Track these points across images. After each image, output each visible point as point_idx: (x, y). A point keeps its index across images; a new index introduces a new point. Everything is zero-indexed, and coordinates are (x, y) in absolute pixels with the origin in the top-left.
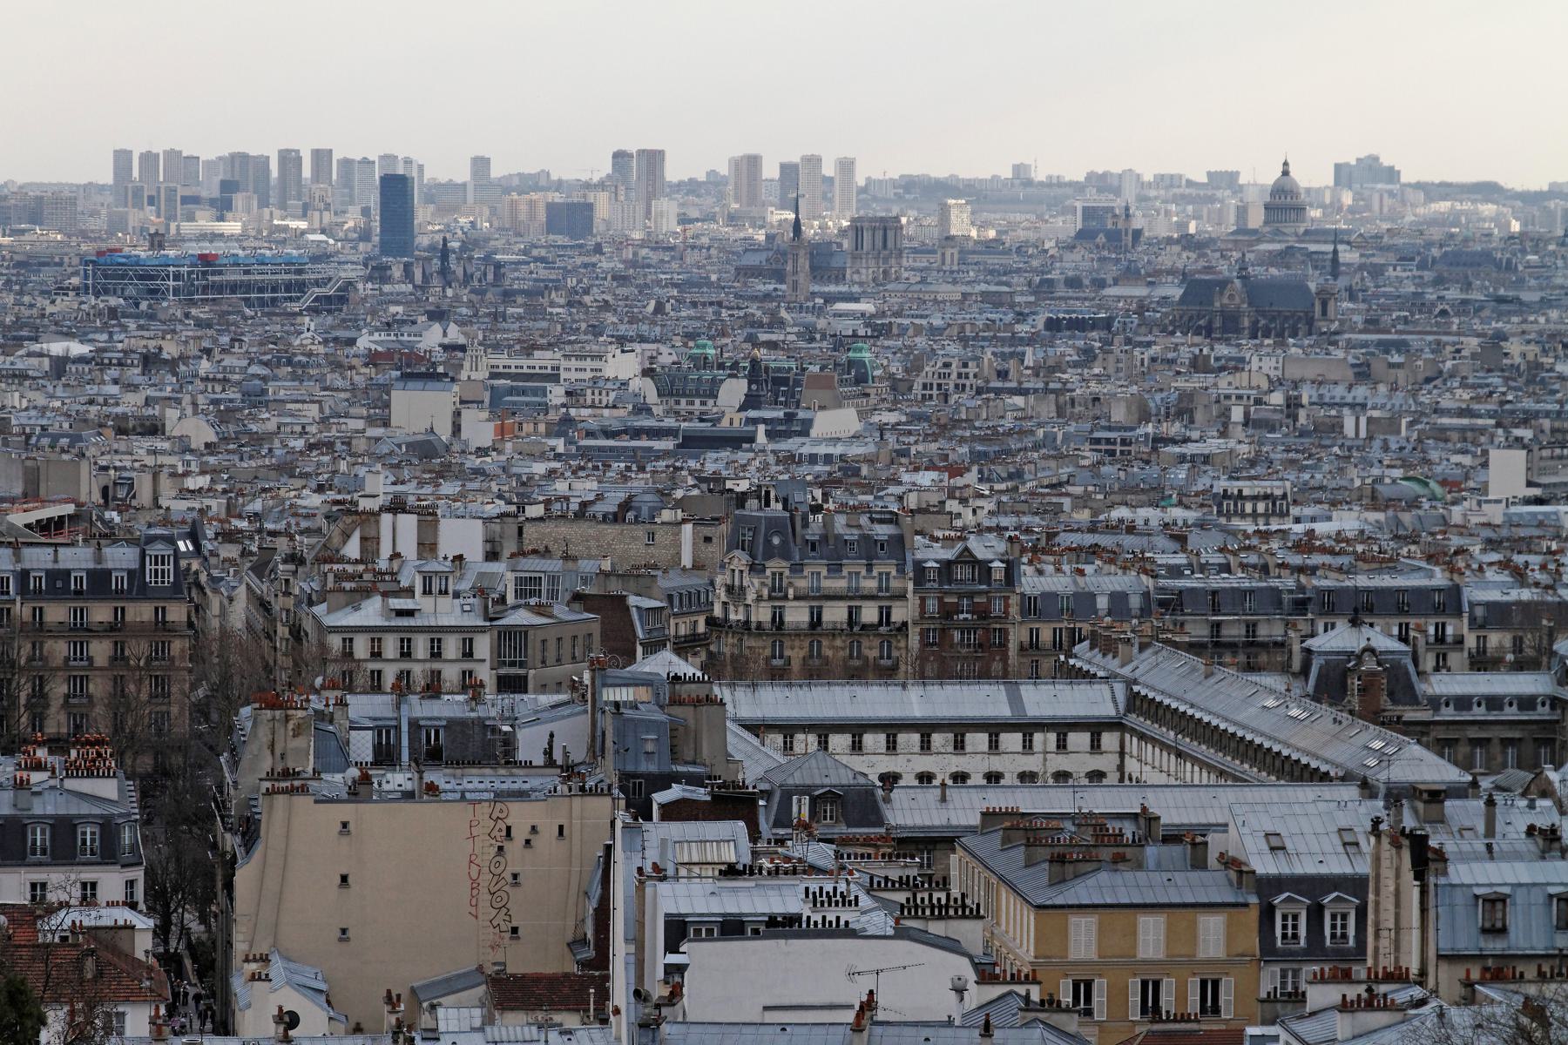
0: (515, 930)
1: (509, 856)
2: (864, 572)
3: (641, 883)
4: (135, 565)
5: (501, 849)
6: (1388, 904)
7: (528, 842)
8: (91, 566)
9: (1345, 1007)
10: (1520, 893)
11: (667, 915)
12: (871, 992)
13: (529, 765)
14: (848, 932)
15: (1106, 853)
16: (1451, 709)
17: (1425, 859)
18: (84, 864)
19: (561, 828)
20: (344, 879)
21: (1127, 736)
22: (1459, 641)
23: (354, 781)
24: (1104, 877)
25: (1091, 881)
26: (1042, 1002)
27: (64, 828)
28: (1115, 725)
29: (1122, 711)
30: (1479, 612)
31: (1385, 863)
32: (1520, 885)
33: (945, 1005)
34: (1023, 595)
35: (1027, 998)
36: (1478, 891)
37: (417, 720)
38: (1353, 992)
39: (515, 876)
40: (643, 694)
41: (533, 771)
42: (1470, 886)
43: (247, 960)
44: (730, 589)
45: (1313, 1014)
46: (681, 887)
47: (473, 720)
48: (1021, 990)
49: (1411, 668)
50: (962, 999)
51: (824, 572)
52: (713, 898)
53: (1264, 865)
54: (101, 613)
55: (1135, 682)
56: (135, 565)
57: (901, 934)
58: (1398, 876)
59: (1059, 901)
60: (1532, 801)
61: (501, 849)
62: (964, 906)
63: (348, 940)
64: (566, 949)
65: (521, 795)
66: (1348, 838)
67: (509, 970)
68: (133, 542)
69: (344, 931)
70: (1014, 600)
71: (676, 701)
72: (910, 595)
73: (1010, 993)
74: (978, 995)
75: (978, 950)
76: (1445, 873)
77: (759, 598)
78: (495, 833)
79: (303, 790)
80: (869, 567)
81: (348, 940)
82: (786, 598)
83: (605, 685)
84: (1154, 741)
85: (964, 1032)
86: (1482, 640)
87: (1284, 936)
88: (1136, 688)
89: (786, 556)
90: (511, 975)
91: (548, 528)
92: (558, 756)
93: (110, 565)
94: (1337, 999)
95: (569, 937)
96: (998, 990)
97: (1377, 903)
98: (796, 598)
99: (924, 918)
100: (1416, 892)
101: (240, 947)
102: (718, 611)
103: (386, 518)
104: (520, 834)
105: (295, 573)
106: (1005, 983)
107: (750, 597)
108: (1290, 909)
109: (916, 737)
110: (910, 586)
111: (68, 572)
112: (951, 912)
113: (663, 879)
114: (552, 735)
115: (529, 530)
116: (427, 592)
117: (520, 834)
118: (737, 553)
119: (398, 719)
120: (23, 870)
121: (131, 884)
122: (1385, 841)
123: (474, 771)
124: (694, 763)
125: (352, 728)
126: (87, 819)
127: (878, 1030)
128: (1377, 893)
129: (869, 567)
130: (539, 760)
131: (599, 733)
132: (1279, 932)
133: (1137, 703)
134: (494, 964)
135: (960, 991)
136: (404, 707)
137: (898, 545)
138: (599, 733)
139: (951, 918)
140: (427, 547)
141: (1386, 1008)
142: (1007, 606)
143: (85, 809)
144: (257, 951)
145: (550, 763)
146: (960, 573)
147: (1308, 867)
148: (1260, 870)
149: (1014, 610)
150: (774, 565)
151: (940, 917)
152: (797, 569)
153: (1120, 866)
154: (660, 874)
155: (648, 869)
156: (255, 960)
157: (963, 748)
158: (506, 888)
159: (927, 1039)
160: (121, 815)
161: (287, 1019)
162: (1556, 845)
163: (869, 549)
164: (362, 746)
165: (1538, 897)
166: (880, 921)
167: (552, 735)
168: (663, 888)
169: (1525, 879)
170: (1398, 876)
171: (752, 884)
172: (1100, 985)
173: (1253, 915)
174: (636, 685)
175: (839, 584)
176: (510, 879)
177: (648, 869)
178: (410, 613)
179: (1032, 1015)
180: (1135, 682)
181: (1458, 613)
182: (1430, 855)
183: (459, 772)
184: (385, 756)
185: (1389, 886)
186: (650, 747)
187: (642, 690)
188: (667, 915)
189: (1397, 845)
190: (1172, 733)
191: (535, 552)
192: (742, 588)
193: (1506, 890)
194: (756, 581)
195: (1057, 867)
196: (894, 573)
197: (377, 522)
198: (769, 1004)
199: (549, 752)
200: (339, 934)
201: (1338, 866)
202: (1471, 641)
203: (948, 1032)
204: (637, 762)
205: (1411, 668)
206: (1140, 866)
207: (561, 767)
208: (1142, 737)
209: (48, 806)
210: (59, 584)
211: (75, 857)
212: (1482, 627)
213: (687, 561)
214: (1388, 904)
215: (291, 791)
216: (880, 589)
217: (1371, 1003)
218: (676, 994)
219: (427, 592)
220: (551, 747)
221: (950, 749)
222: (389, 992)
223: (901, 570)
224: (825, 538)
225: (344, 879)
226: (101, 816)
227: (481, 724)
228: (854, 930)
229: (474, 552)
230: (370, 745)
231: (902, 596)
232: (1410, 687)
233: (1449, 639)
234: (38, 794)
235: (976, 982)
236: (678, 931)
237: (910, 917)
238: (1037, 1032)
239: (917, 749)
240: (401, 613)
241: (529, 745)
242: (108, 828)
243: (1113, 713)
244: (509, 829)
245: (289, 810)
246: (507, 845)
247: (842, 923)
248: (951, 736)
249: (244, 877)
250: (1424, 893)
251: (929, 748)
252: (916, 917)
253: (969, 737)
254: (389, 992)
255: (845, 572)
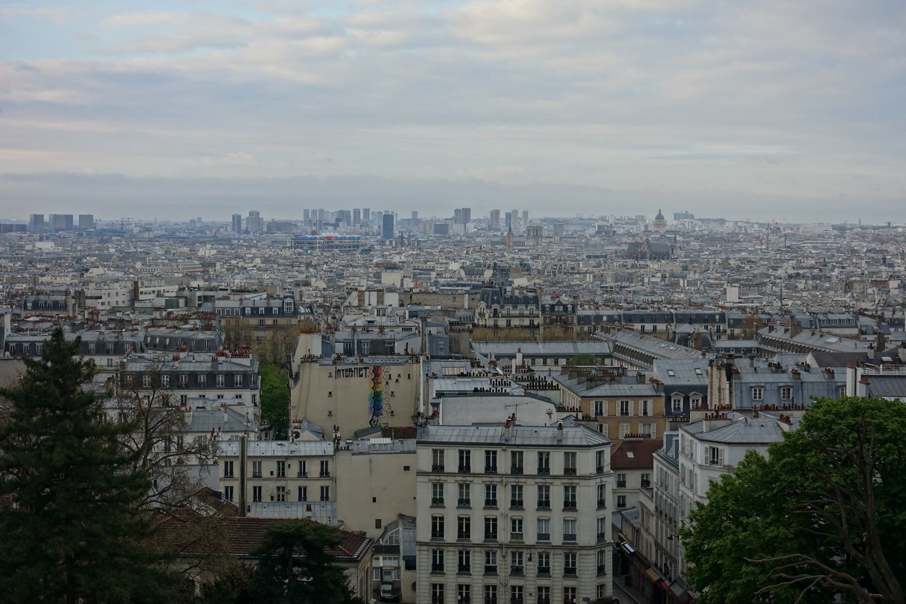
0: (392, 412)
1: (390, 385)
2: (525, 308)
3: (427, 380)
4: (281, 306)
5: (387, 383)
6: (716, 392)
7: (397, 380)
8: (266, 306)
9: (707, 418)
10: (768, 385)
11: (436, 391)
12: (514, 414)
13: (399, 354)
14: (506, 394)
15: (607, 379)
16: (723, 352)
17: (731, 373)
18: (237, 389)
19: (409, 375)
20: (330, 393)
21: (614, 360)
22: (725, 331)
23: (335, 359)
24: (607, 386)
25: (602, 388)
26: (583, 417)
27: (229, 375)
28: (609, 356)
29: (612, 350)
30: (731, 322)
31: (715, 376)
32: (768, 383)
33: (543, 419)
34: (578, 316)
35: (577, 417)
36: (751, 385)
37: (361, 340)
38: (709, 413)
39: (392, 393)
40: (441, 329)
41: (400, 357)
42: (749, 383)
43: (294, 422)
44: (480, 314)
45: (692, 423)
46: (442, 381)
47: (380, 340)
48: (574, 414)
49: (710, 339)
50: (551, 417)
51: (511, 308)
52: (455, 385)
53: (668, 382)
54: (269, 321)
55: (616, 341)
56: (281, 306)
57: (527, 395)
58: (720, 381)
59: (590, 394)
60: (767, 359)
61: (387, 383)
62: (552, 386)
63: (331, 416)
64: (411, 419)
65: (396, 364)
66: (698, 371)
67: (389, 426)
68: (280, 299)
69: (330, 412)
70: (575, 318)
71: (452, 330)
72: (540, 316)
73: (570, 416)
74: (557, 417)
75: (557, 402)
76: (739, 378)
77: (490, 317)
78: (385, 377)
79: (316, 361)
80: (527, 307)
81: (331, 416)
82: (498, 317)
83: (426, 326)
84: (623, 360)
85: (551, 429)
86: (732, 331)
87: (675, 408)
88: (616, 343)
89: (498, 303)
90: (389, 428)
91: (421, 296)
92: (409, 351)
93: (272, 306)
94: (704, 416)
95: (412, 414)
96: (565, 415)
97: (711, 393)
98: (502, 317)
99: (536, 389)
100: (728, 386)
101: (292, 418)
102: (476, 321)
103: (367, 293)
104: (394, 377)
105: (337, 311)
106: (568, 411)
107: (487, 316)
108: (677, 398)
109: (542, 360)
110: (540, 313)
111: (258, 308)
112: (547, 388)
113: (436, 378)
114: (407, 344)
115: (414, 297)
116: (378, 315)
117: (394, 377)
118: (482, 302)
119: (354, 340)
120: (215, 390)
121: (254, 396)
122: (715, 368)
123: (380, 357)
124: (458, 353)
125: (336, 342)
126: (238, 372)
127: (515, 428)
128: (712, 388)
129: (527, 307)
130: (403, 353)
131: (424, 343)
132: (672, 406)
133: (617, 348)
134: (384, 424)
135: (550, 414)
136: (356, 335)
137: (536, 300)
138: (424, 343)
139: (547, 390)
140: (380, 301)
141: (724, 419)
142: (573, 320)
143: (237, 369)
144: (300, 418)
145: (407, 354)
146: (556, 308)
147: (684, 382)
148: (665, 384)
149: (575, 321)
150: (495, 306)
151: (542, 390)
152: (502, 307)
153: (613, 382)
154: (435, 376)
155: (430, 375)
156: (297, 422)
157: (557, 364)
158: (390, 397)
159: (536, 432)
160: (250, 371)
161: (294, 435)
162: (780, 370)
163: (526, 301)
164: (339, 348)
165: (775, 387)
166: (521, 391)
167: (407, 344)
168: (436, 381)
169: (770, 381)
170: (720, 381)
171: (470, 380)
172: (605, 427)
173: (663, 400)
174: (438, 326)
175: (517, 312)
176: (390, 394)
177: (430, 375)
178: (373, 322)
179: (579, 422)
180: (616, 341)
181: (724, 322)
182: (733, 372)
183: (374, 357)
184: (349, 352)
185: (716, 385)
186: (441, 347)
187: (440, 327)
188: (436, 391)
189: (719, 369)
190: (629, 358)
191: (415, 304)
192: (484, 313)
193: (763, 385)
194: (488, 311)
195: (589, 383)
196: (535, 308)
197: (364, 294)
198: (474, 422)
199: (406, 350)
200: (328, 414)
201: (695, 382)
202: (729, 332)
203: (545, 429)
204: (437, 352)
205: (710, 339)
206: (620, 383)
207: (410, 355)
208: (618, 359)
209: (224, 368)
210: (255, 312)
211: (233, 386)
212: (732, 327)
213: (466, 306)
214: (716, 392)
215: (312, 361)
216: (530, 314)
217: (717, 418)
218: (435, 414)
219: (378, 315)
220: (407, 347)
221: (553, 364)
222: (335, 426)
223: (537, 308)
224: (511, 297)
225: (330, 393)
226: (243, 371)
227: (383, 342)
228: (508, 393)
229: (396, 304)
230: (342, 348)
231: (538, 316)
232: (709, 345)
233: (721, 331)
234: (221, 363)
235: (557, 411)
236: (440, 394)
237: (531, 389)
238: (581, 429)
239: (542, 364)
240: (369, 322)
241: (399, 348)
242: (245, 375)
243: (608, 352)
244: (390, 375)
245: (310, 366)
246: (389, 381)
247: (504, 391)
248: (553, 360)
249: (294, 393)
250: (730, 386)
251: (546, 364)
252: (533, 389)
253: (559, 360)
254: (335, 426)
255: (518, 308)
